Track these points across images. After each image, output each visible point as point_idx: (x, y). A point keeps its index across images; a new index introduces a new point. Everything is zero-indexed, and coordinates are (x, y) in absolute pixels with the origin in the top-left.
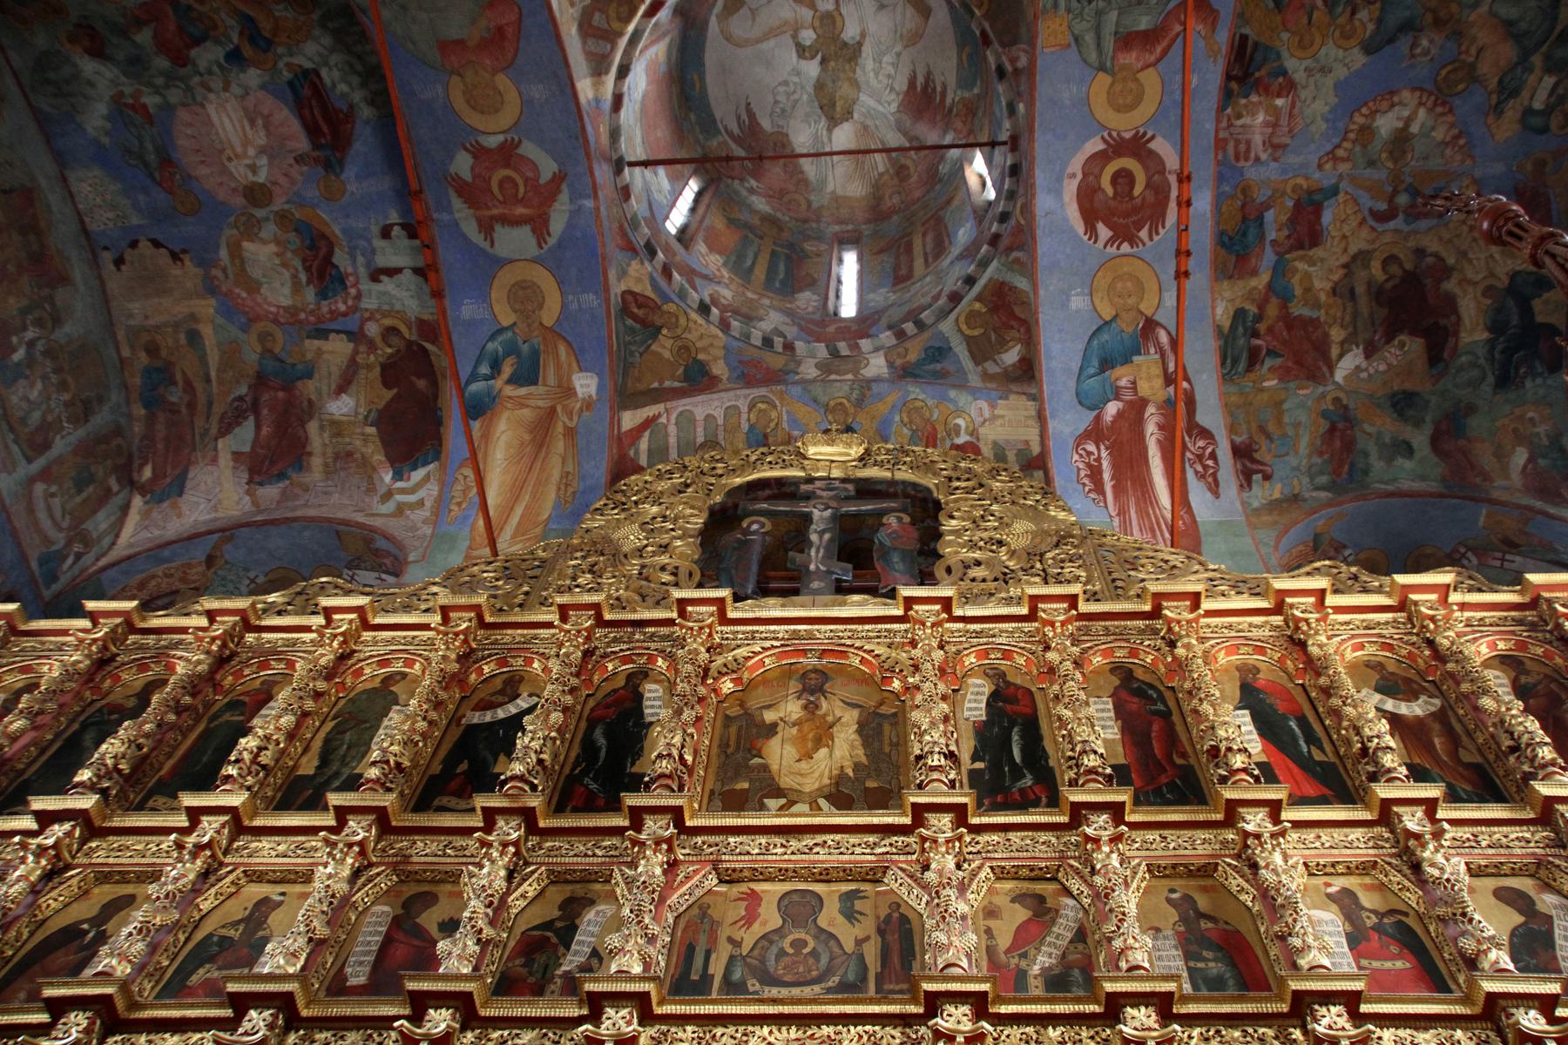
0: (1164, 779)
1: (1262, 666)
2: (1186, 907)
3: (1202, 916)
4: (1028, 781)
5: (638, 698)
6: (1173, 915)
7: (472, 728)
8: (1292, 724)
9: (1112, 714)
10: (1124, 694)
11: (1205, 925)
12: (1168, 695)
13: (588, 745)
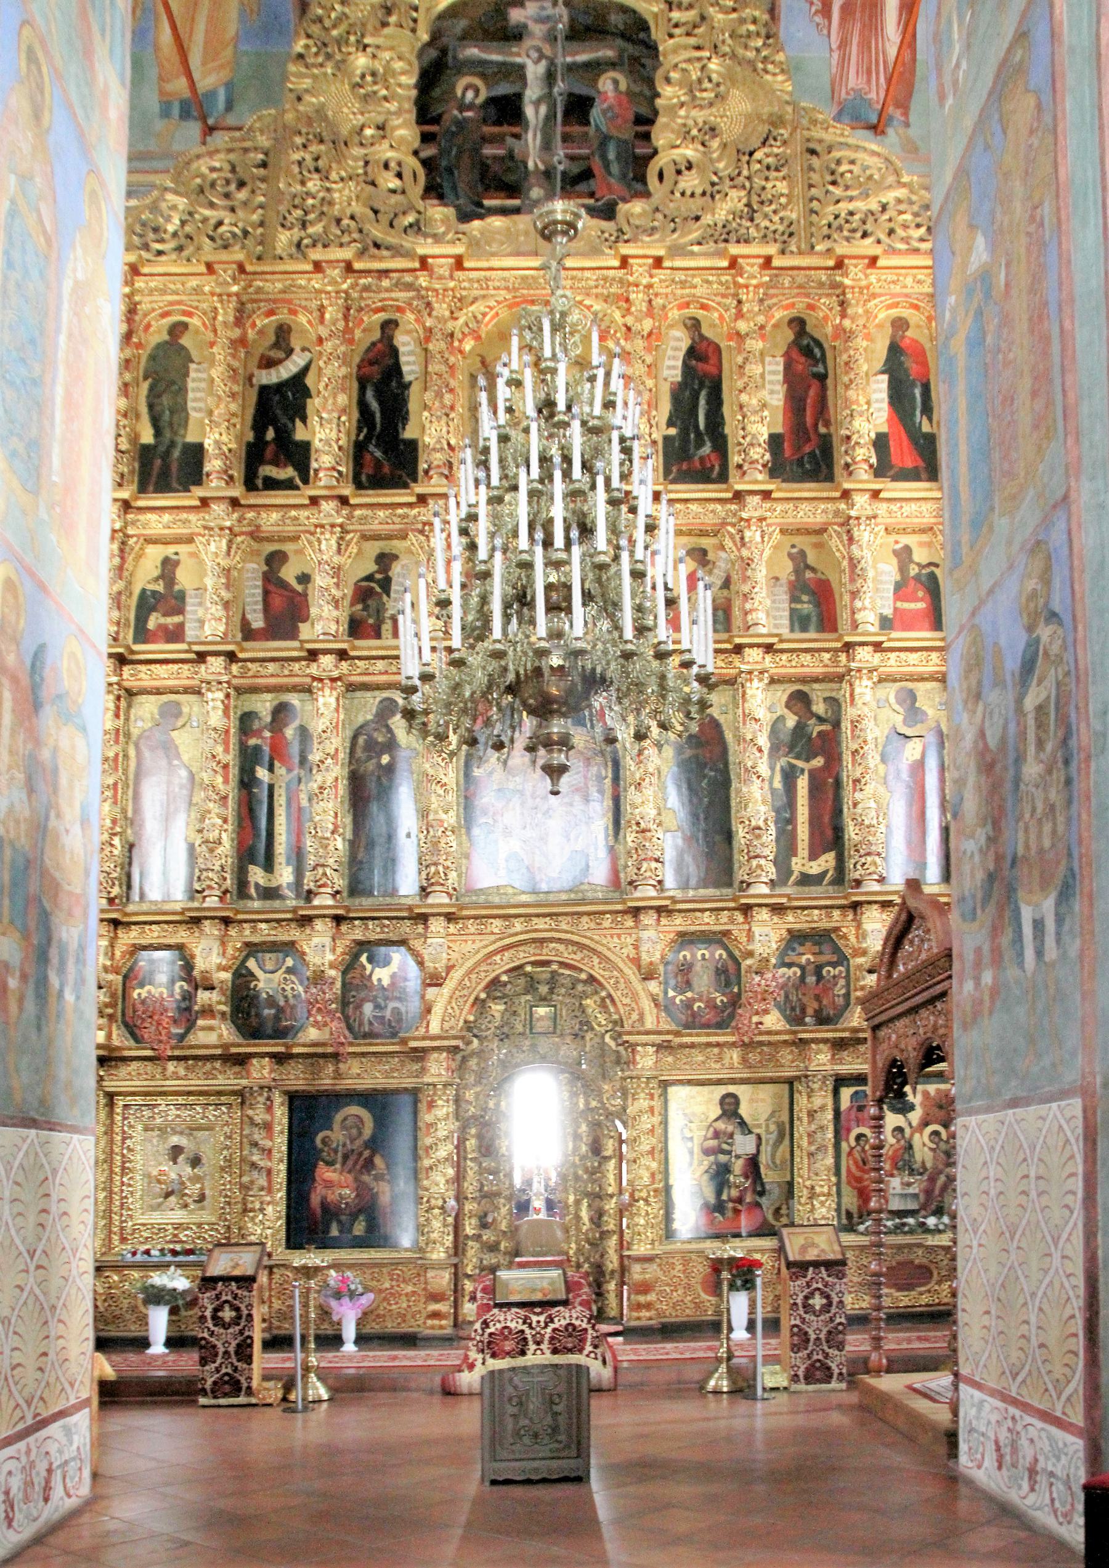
0: (807, 449)
1: (912, 323)
2: (800, 560)
3: (808, 567)
4: (707, 449)
5: (394, 352)
6: (789, 566)
7: (264, 390)
8: (917, 392)
9: (780, 377)
10: (795, 355)
11: (809, 575)
12: (829, 355)
13: (363, 405)
